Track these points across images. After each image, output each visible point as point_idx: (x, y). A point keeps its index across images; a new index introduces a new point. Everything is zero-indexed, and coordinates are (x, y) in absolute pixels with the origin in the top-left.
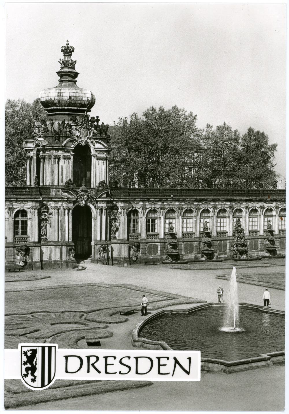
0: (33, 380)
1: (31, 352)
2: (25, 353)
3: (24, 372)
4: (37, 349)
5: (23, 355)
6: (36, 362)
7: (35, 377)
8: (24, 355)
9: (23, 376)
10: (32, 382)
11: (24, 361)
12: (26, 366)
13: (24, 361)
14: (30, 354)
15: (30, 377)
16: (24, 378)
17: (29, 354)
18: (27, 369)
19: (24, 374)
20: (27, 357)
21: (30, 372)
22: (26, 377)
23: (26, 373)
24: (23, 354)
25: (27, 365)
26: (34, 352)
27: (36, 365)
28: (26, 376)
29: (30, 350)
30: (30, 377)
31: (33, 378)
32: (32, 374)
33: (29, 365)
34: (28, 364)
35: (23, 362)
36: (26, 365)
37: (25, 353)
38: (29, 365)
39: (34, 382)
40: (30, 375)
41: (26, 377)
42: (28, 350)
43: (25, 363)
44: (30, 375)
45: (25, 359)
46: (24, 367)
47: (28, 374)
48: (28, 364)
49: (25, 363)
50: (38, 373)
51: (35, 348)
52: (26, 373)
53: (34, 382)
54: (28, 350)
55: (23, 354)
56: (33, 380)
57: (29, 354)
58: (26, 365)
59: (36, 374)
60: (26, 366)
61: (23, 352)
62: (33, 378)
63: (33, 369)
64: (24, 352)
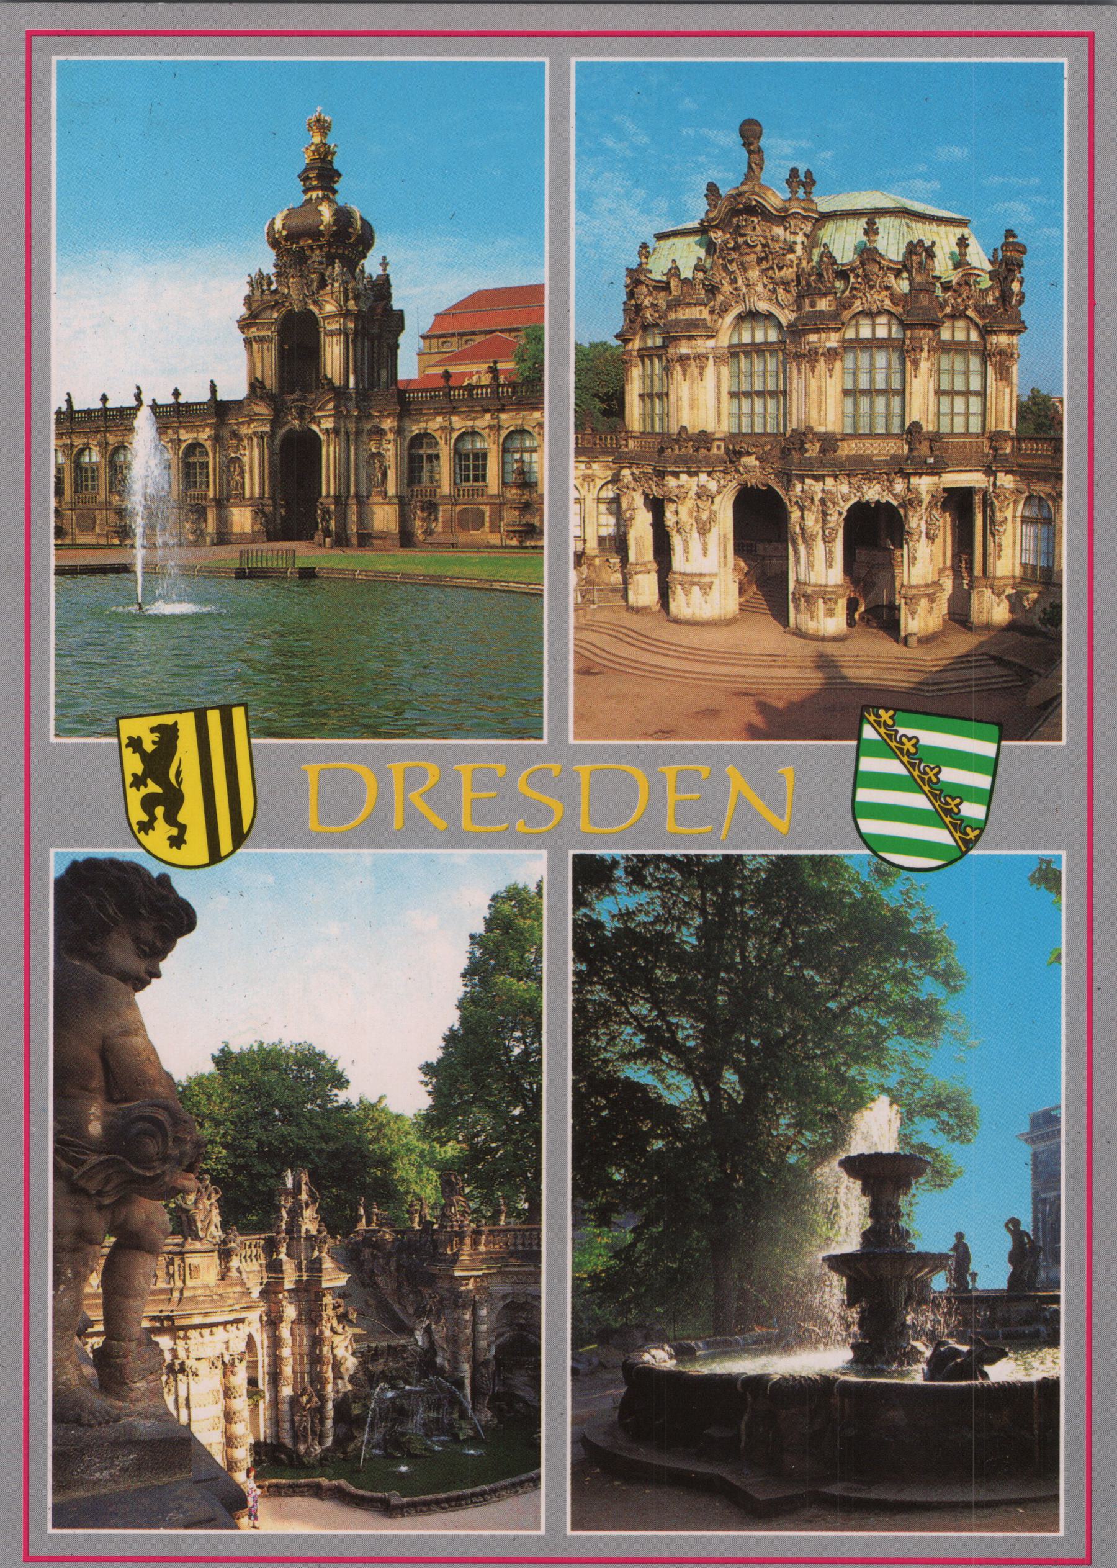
0: (177, 842)
1: (155, 737)
3: (138, 814)
4: (176, 723)
5: (127, 752)
6: (178, 773)
7: (183, 828)
8: (131, 750)
9: (136, 828)
10: (171, 846)
11: (134, 775)
12: (144, 791)
13: (134, 775)
14: (154, 742)
15: (162, 830)
16: (142, 836)
17: (149, 747)
18: (148, 804)
19: (140, 823)
20: (144, 756)
21: (159, 811)
22: (147, 833)
24: (128, 746)
25: (146, 786)
26: (168, 736)
27: (179, 784)
28: (146, 827)
30: (162, 830)
31: (175, 832)
32: (171, 819)
33: (153, 788)
34: (149, 781)
35: (129, 779)
36: (142, 788)
38: (153, 788)
39: (179, 848)
40: (161, 825)
41: (147, 833)
43: (138, 782)
44: (161, 825)
45: (134, 764)
46: (135, 797)
47: (153, 818)
48: (149, 781)
49: (138, 782)
50: (192, 812)
51: (168, 720)
53: (179, 848)
55: (128, 746)
56: (177, 842)
57: (149, 747)
58: (142, 788)
59: (182, 818)
60: (144, 791)
61: (125, 741)
62: (175, 832)
63: (172, 800)
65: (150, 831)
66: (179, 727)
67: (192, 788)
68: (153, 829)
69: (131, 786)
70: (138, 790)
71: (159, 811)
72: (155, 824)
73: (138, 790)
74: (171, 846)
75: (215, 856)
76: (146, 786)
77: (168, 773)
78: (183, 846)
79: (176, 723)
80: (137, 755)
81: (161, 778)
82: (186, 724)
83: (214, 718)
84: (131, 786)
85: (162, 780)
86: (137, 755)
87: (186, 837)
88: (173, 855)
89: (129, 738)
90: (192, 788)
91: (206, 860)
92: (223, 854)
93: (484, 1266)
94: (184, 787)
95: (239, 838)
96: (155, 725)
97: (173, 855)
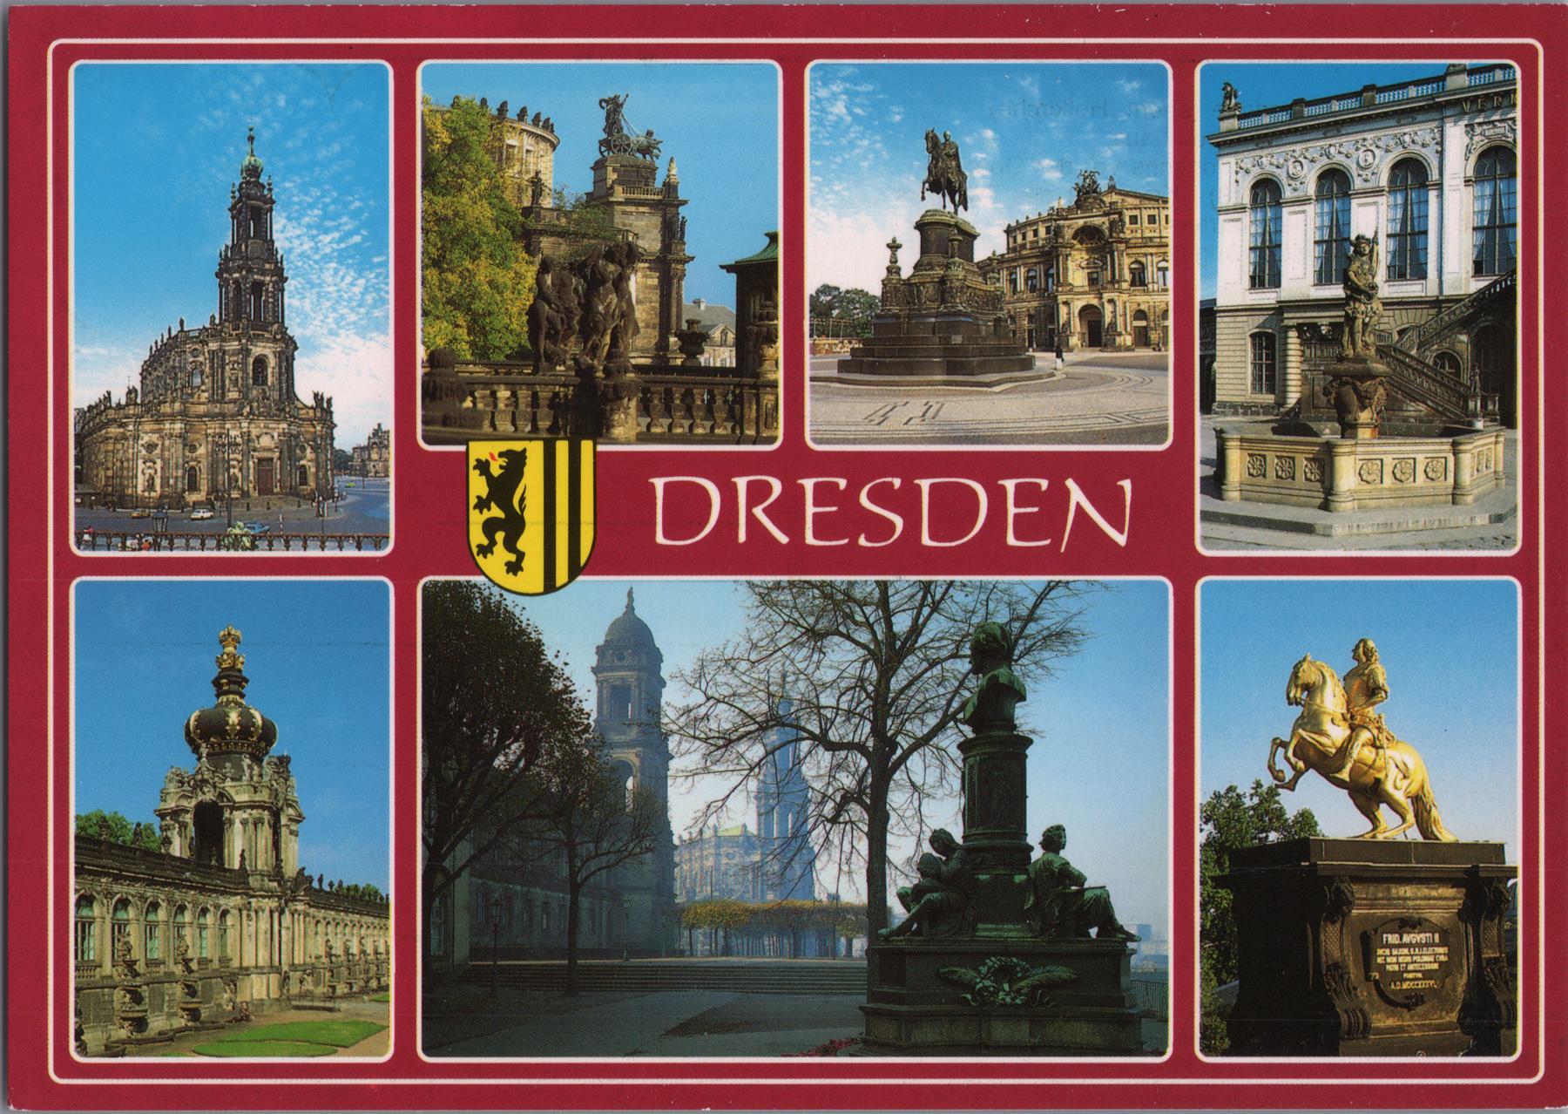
0: (514, 568)
1: (503, 461)
2: (483, 467)
4: (525, 450)
6: (522, 499)
8: (478, 472)
9: (475, 550)
10: (508, 572)
11: (479, 497)
12: (487, 514)
13: (479, 497)
14: (501, 467)
15: (501, 555)
17: (496, 471)
18: (490, 527)
19: (480, 546)
21: (500, 536)
22: (485, 557)
23: (485, 542)
24: (475, 468)
25: (489, 509)
26: (516, 462)
27: (522, 510)
28: (485, 550)
29: (501, 455)
30: (501, 555)
31: (512, 557)
32: (510, 545)
33: (496, 512)
34: (493, 505)
36: (485, 511)
37: (483, 467)
38: (496, 512)
39: (515, 574)
40: (499, 548)
41: (485, 557)
42: (492, 456)
43: (482, 504)
44: (499, 548)
47: (493, 543)
48: (493, 505)
49: (482, 504)
50: (532, 541)
51: (517, 446)
52: (485, 542)
53: (515, 574)
54: (492, 456)
55: (475, 468)
56: (514, 568)
57: (496, 471)
58: (485, 511)
59: (521, 544)
60: (487, 514)
62: (512, 557)
63: (513, 526)
64: (478, 461)
65: (489, 555)
66: (527, 454)
67: (534, 515)
68: (492, 553)
69: (475, 508)
70: (481, 512)
71: (500, 536)
72: (495, 549)
73: (481, 512)
74: (508, 572)
75: (550, 586)
76: (489, 509)
77: (512, 499)
78: (520, 573)
79: (525, 450)
80: (484, 477)
81: (506, 505)
82: (535, 451)
83: (562, 448)
84: (475, 508)
85: (506, 505)
86: (484, 477)
87: (523, 565)
88: (509, 581)
89: (478, 460)
90: (534, 515)
91: (541, 589)
92: (558, 584)
93: (1030, 935)
94: (526, 514)
95: (575, 570)
96: (504, 449)
97: (509, 581)
